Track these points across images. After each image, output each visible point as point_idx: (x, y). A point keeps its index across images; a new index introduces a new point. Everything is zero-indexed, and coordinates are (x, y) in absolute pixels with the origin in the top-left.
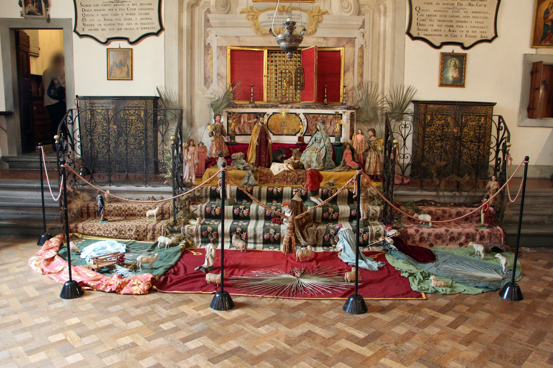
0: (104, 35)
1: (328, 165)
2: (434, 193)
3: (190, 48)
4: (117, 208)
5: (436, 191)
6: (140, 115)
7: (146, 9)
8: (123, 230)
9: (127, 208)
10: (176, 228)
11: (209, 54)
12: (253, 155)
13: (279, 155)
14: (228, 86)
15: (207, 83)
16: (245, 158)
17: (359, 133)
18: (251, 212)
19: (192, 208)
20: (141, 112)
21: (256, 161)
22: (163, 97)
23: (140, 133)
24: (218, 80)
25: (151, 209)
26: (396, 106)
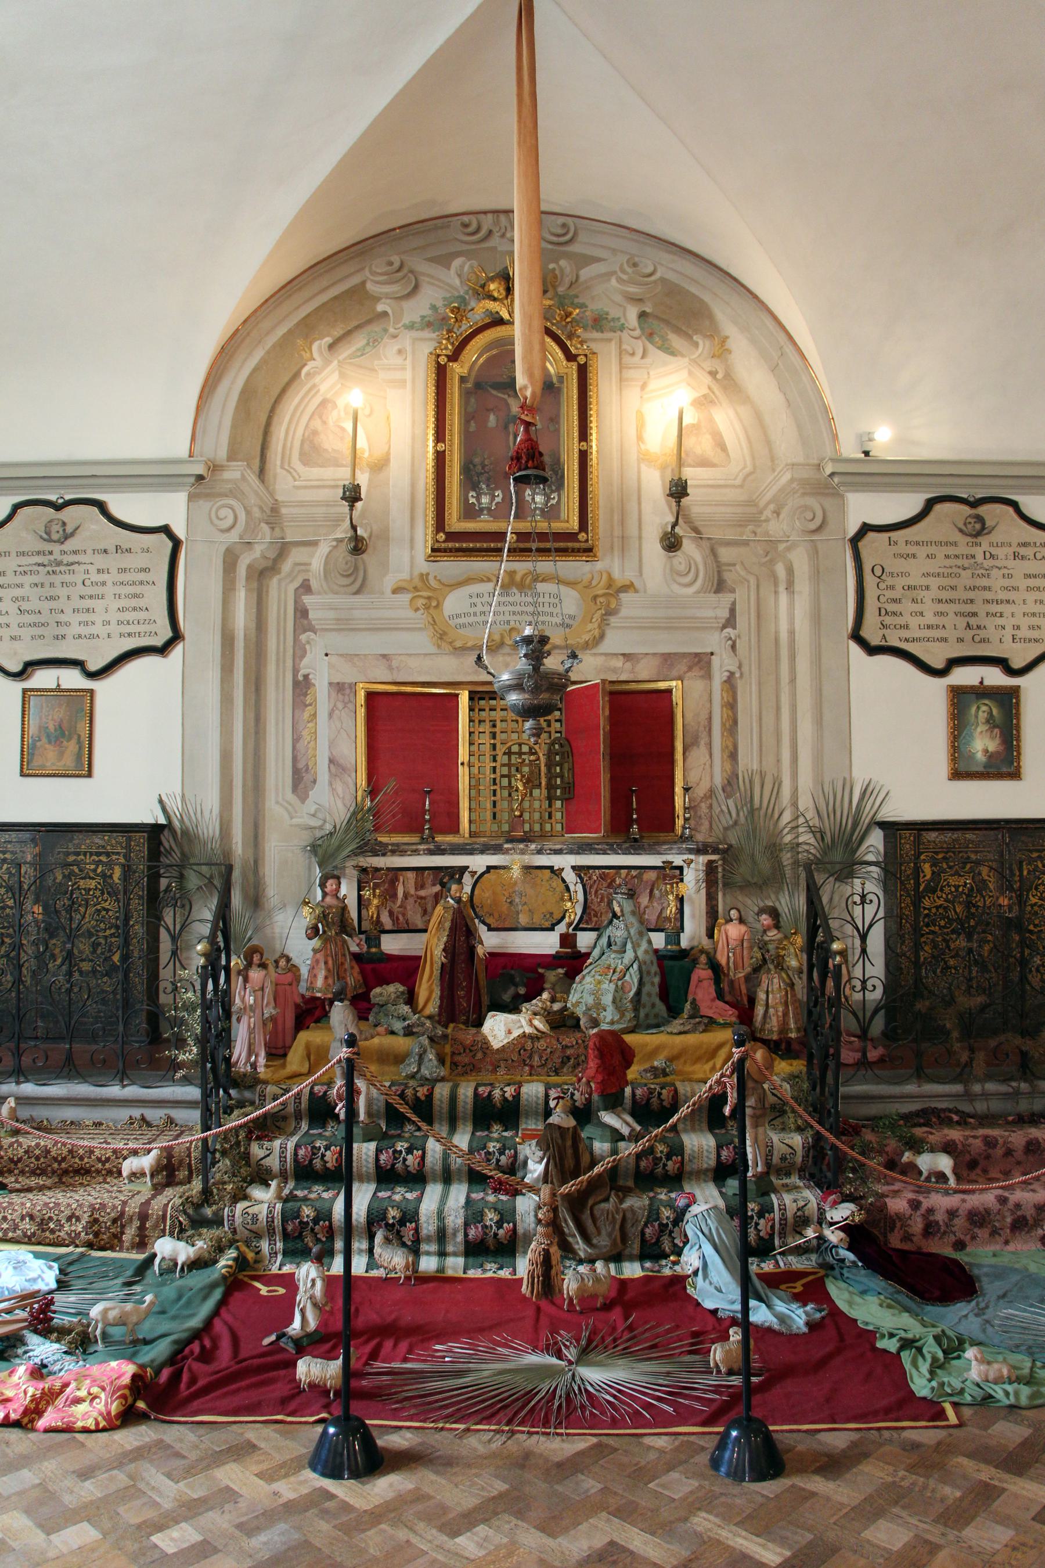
0: (15, 654)
1: (647, 1016)
2: (957, 1088)
3: (253, 689)
4: (37, 1152)
5: (961, 1082)
6: (111, 877)
7: (134, 583)
8: (50, 1218)
9: (65, 1152)
10: (208, 1212)
11: (306, 706)
12: (431, 992)
13: (505, 991)
14: (360, 793)
15: (301, 786)
16: (411, 999)
17: (731, 920)
18: (429, 1159)
19: (257, 1150)
20: (113, 869)
21: (440, 1007)
22: (177, 824)
23: (110, 928)
24: (333, 776)
25: (135, 1153)
26: (833, 840)
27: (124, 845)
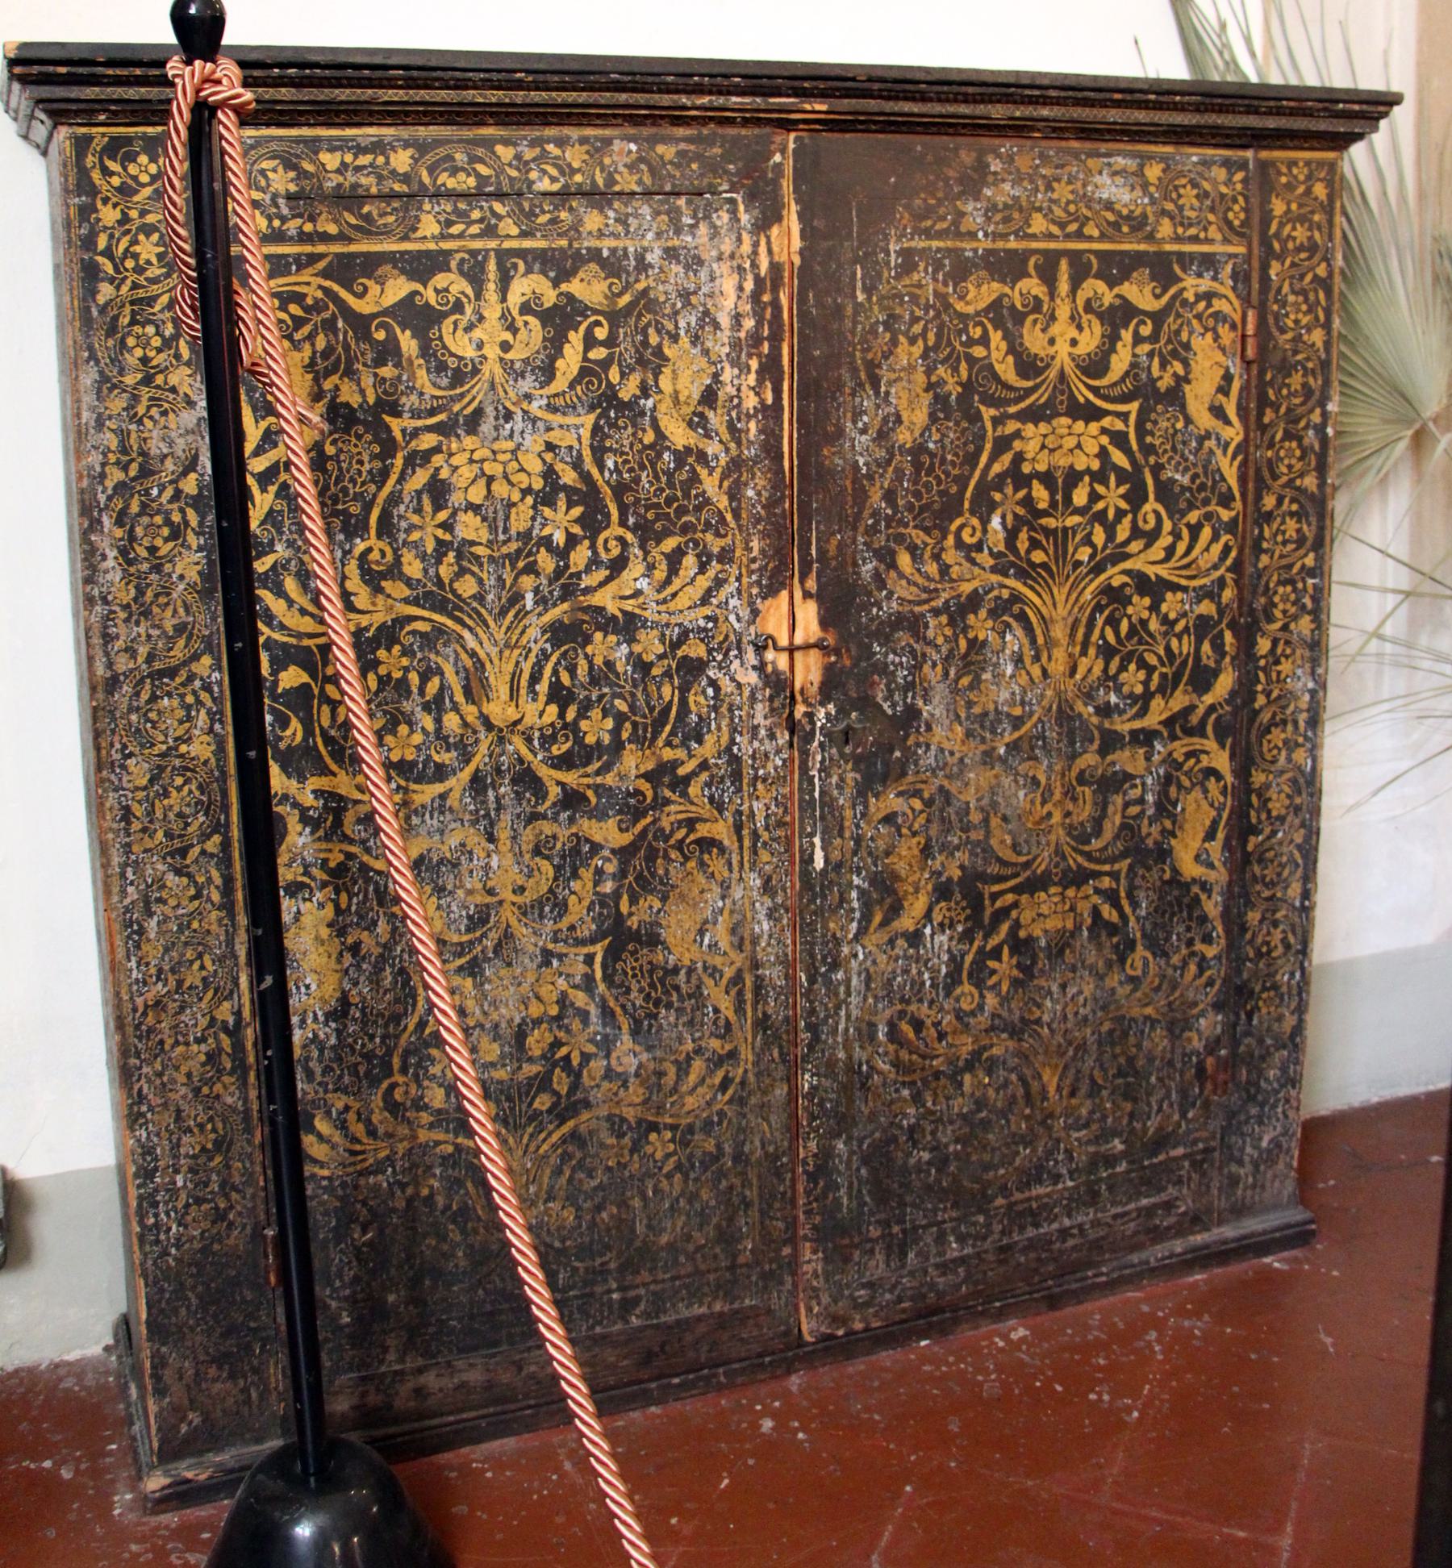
6: (1175, 397)
20: (1181, 352)
23: (1167, 688)
27: (1236, 216)
